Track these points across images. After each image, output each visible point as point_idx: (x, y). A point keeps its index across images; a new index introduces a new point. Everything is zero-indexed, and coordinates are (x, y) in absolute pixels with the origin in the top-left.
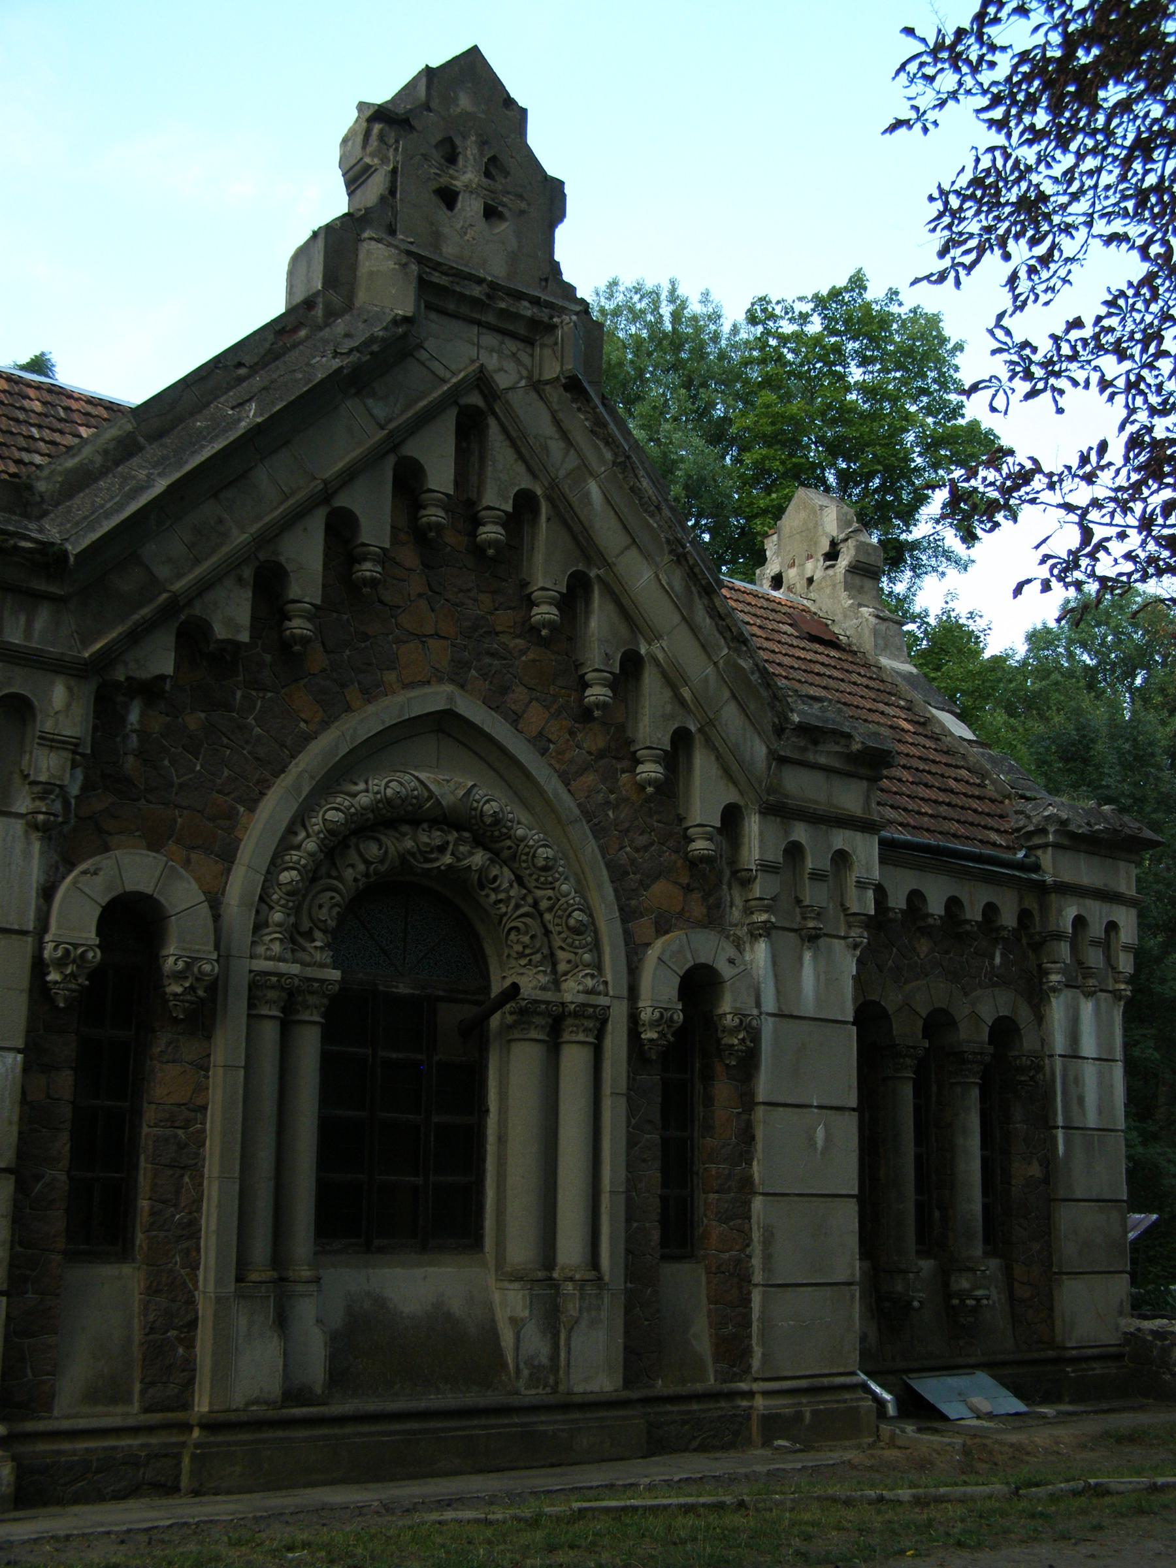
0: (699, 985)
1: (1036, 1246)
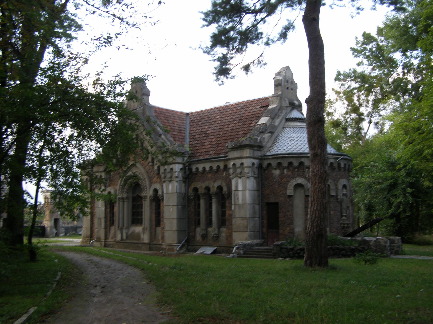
0: (156, 191)
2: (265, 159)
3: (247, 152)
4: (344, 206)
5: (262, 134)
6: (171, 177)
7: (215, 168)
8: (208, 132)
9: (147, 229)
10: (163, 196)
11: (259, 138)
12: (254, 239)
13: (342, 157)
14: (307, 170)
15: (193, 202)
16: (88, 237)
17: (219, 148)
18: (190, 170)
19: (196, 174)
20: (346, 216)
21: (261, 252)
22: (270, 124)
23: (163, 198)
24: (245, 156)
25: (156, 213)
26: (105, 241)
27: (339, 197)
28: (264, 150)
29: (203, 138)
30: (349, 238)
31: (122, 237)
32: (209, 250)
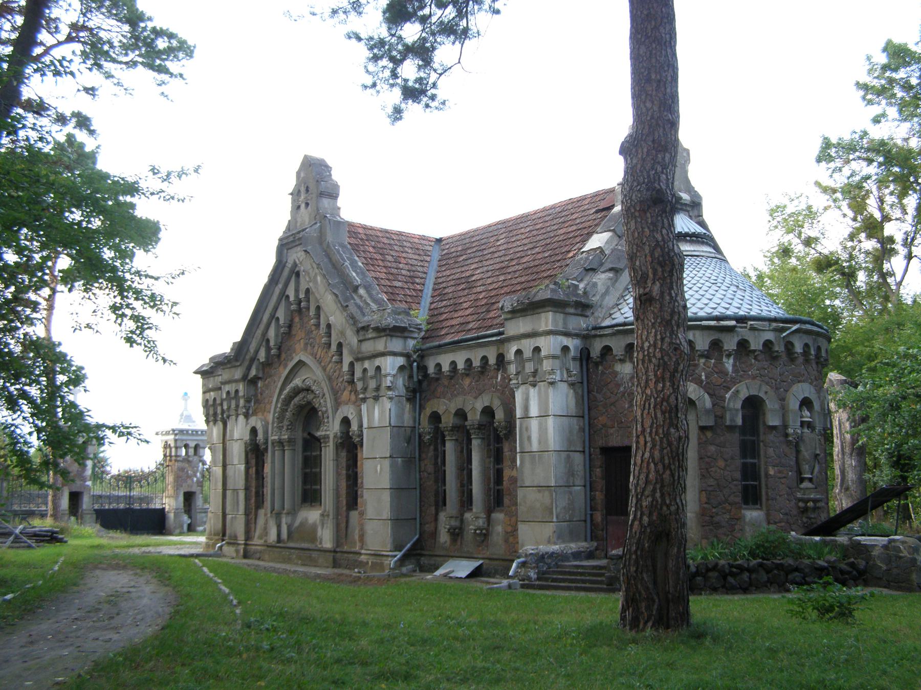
0: (346, 422)
1: (514, 508)
2: (595, 336)
3: (548, 320)
4: (806, 453)
5: (591, 273)
6: (378, 389)
7: (476, 363)
8: (473, 278)
9: (328, 516)
10: (361, 435)
11: (582, 286)
12: (572, 540)
13: (795, 327)
14: (702, 361)
15: (432, 447)
16: (218, 535)
17: (492, 314)
18: (423, 369)
19: (437, 379)
20: (810, 480)
21: (581, 574)
22: (613, 250)
23: (362, 439)
24: (543, 328)
25: (348, 477)
26: (246, 544)
27: (790, 431)
28: (596, 314)
29: (461, 294)
30: (817, 538)
31: (279, 535)
32: (462, 568)
